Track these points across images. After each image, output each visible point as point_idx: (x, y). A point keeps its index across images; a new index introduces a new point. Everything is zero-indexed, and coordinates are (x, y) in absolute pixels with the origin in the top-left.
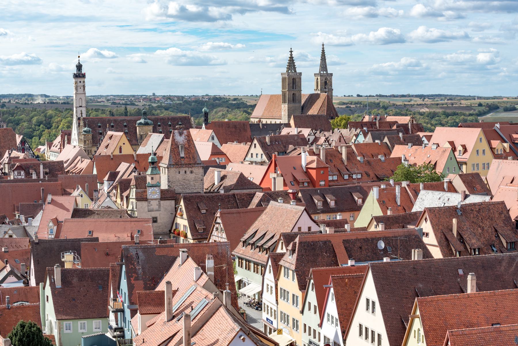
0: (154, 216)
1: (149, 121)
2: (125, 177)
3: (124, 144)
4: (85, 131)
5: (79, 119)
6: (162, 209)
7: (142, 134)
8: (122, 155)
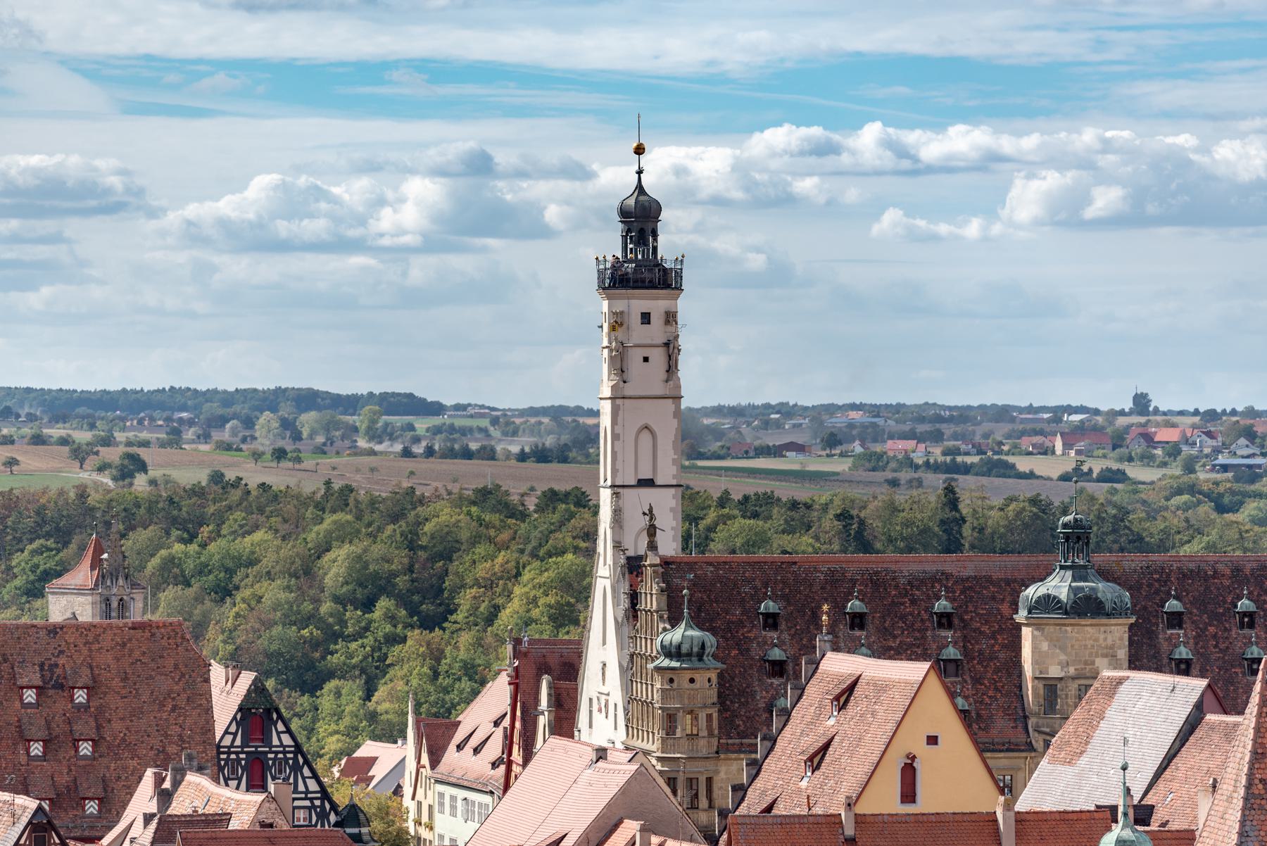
1: (1104, 590)
3: (933, 740)
4: (672, 652)
5: (633, 566)
7: (1054, 672)
8: (920, 819)
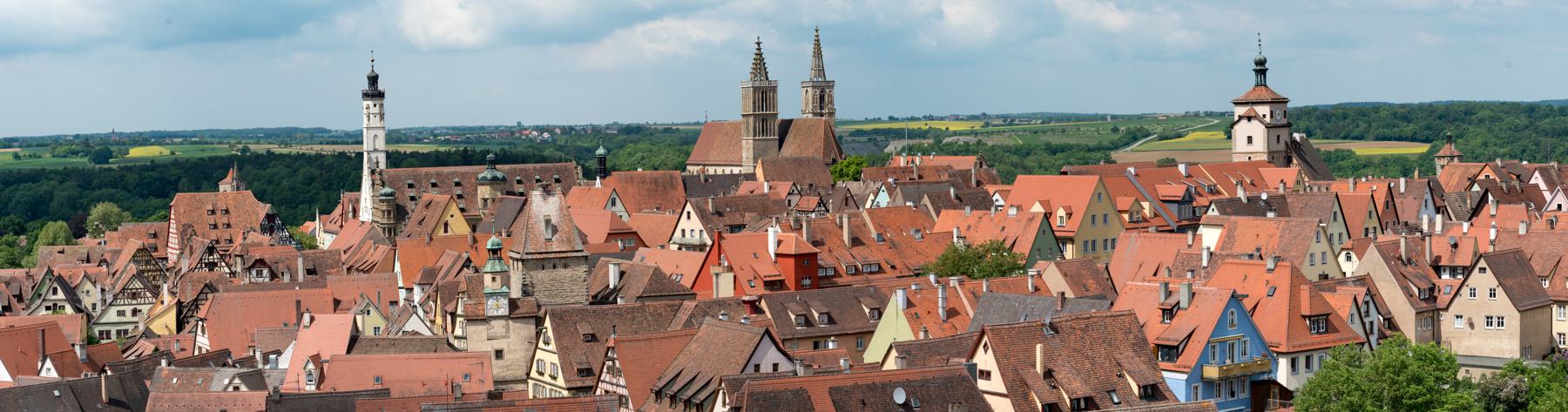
0: (499, 347)
2: (451, 277)
5: (373, 172)
6: (512, 334)
